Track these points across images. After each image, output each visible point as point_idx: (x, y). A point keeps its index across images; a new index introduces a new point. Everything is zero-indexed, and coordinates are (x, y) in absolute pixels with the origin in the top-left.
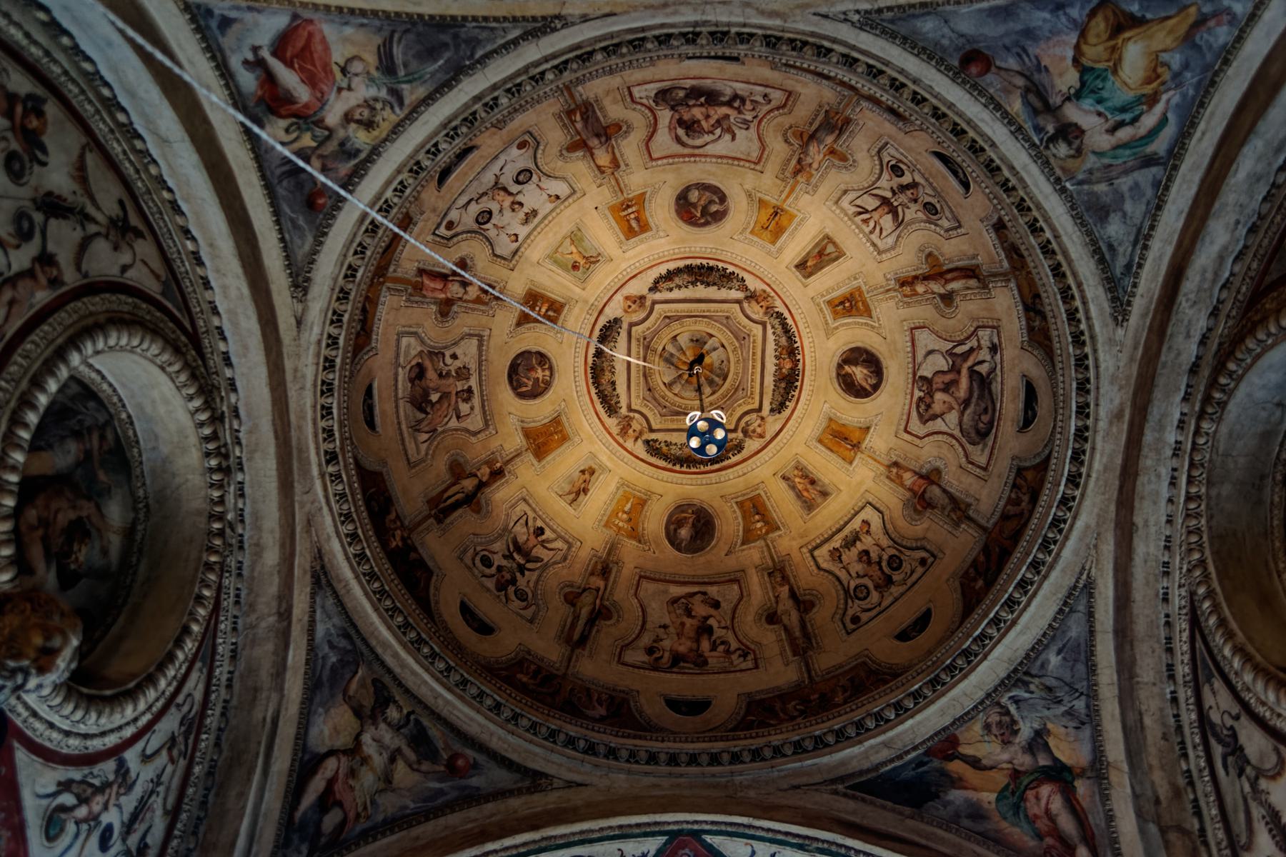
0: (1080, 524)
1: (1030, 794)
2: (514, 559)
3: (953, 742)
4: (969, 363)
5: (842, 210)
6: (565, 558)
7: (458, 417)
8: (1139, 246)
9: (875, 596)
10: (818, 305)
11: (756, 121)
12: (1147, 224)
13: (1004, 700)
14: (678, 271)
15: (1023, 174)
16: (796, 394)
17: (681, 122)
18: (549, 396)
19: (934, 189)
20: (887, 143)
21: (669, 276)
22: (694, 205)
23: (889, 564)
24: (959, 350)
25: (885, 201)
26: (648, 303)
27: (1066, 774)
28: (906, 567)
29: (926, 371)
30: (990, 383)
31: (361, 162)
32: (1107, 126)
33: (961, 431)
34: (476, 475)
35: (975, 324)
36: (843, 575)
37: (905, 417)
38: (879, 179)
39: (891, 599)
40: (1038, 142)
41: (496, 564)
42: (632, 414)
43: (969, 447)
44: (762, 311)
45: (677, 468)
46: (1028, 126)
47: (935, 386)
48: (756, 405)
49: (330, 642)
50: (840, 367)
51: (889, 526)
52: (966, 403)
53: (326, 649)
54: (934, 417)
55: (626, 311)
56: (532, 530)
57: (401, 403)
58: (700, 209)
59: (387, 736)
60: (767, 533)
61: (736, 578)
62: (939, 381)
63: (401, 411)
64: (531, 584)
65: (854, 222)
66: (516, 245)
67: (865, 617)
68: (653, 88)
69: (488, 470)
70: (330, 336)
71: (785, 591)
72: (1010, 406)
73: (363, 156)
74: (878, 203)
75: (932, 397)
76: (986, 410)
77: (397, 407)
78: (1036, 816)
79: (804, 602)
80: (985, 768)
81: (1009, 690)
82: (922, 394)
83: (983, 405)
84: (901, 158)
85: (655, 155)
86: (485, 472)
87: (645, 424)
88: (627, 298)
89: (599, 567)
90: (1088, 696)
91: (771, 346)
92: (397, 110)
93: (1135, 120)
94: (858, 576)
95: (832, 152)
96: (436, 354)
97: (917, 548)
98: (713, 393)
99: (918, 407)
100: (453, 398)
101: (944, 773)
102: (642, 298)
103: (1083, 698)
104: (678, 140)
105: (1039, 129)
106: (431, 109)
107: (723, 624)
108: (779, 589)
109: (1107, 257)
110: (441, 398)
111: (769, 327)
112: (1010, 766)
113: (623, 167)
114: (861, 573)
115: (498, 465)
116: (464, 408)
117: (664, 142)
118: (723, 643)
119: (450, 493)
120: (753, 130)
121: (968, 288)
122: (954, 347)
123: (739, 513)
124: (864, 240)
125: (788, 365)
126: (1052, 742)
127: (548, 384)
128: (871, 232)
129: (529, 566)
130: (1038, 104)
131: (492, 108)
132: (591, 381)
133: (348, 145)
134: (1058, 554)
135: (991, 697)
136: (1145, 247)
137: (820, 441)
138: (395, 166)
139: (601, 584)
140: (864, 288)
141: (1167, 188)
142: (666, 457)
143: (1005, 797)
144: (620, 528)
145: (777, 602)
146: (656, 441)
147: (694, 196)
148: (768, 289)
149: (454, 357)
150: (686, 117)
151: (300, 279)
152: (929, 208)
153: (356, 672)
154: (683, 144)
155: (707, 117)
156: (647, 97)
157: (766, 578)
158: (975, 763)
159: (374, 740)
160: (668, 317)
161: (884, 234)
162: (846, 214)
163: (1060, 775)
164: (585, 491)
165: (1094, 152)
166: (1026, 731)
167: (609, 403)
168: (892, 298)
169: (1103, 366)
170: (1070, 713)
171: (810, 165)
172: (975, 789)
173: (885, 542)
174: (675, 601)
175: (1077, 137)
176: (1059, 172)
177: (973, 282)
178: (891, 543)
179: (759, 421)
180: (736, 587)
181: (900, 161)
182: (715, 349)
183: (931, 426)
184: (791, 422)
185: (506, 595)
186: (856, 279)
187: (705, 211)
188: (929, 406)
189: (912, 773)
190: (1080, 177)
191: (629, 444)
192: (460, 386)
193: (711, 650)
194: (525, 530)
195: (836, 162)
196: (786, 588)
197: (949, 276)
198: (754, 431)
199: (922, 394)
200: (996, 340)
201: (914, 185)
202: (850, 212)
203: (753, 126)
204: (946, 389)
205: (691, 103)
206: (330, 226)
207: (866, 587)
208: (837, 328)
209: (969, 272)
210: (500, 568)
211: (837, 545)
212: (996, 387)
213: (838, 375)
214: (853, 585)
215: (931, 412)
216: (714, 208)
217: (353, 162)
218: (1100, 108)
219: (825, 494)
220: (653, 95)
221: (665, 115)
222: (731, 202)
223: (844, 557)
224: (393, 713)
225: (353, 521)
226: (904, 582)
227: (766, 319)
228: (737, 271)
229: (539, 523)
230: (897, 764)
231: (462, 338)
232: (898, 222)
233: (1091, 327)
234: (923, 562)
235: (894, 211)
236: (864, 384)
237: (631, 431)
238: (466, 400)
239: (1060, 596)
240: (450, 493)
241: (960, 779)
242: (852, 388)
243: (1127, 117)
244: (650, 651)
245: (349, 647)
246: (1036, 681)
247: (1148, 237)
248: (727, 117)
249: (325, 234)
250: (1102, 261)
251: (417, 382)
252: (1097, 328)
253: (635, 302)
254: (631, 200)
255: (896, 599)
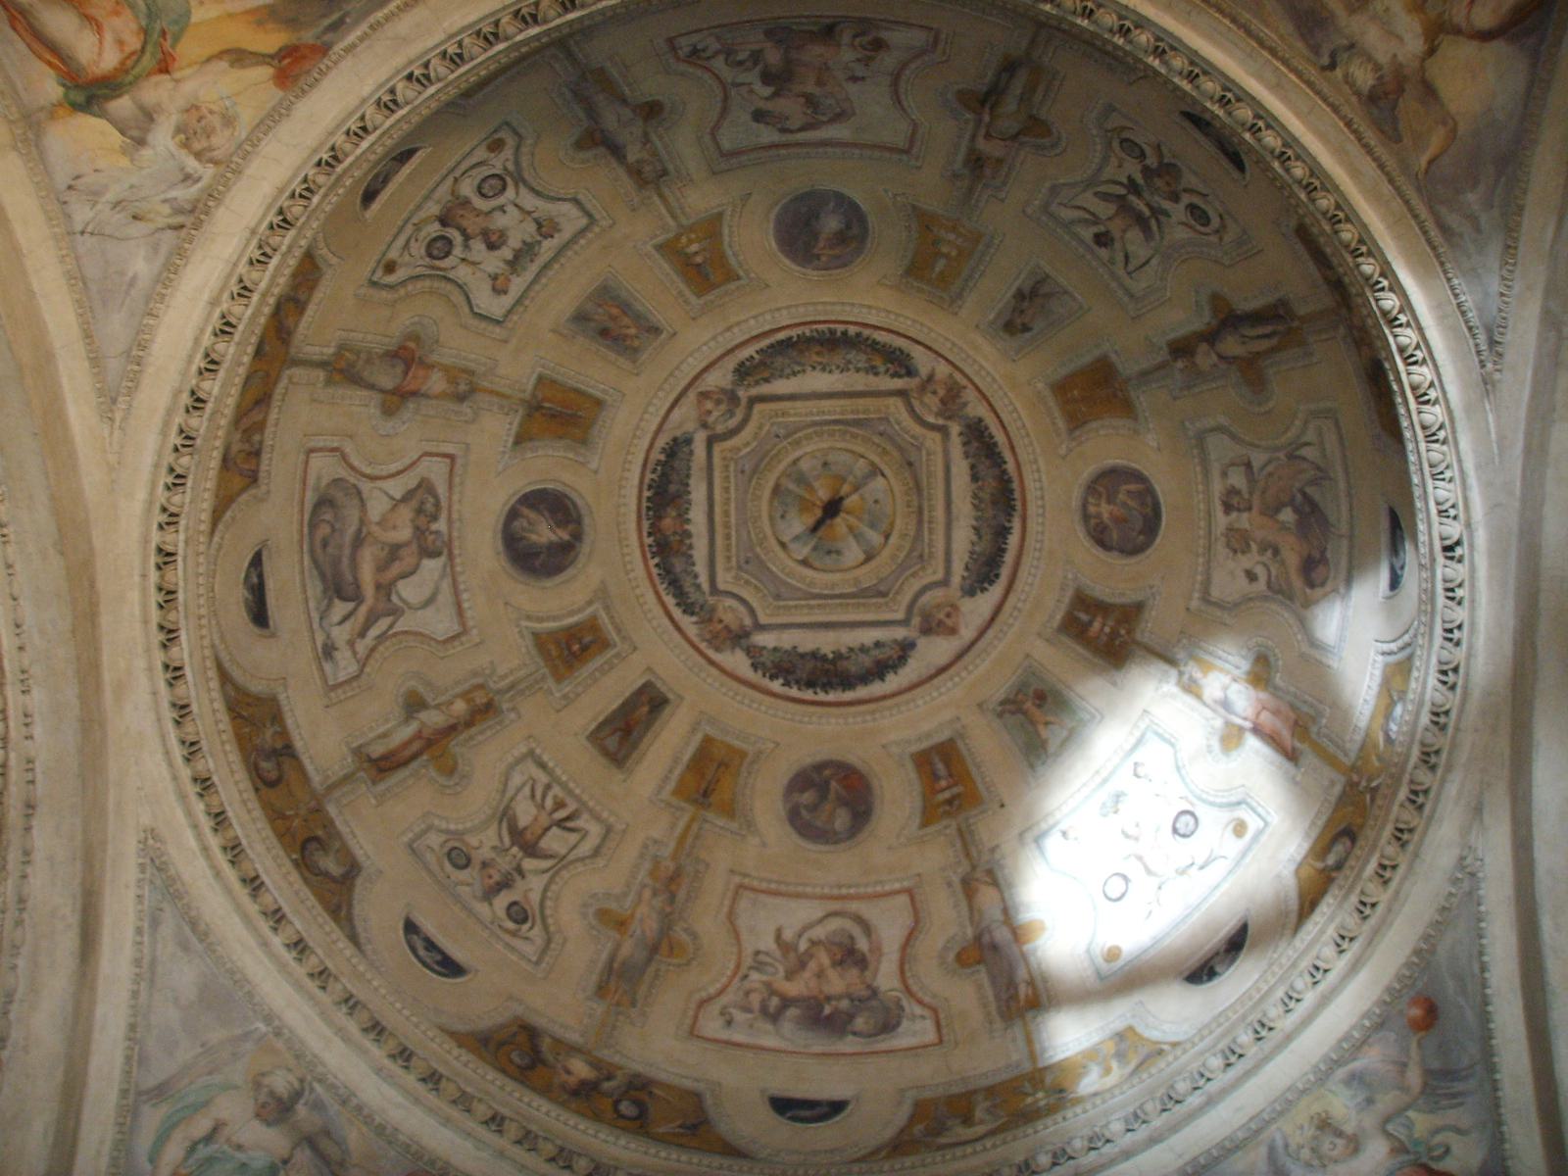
0: (141, 495)
1: (134, 43)
2: (1148, 205)
3: (283, 79)
4: (363, 609)
5: (597, 818)
6: (1054, 190)
7: (1248, 465)
8: (146, 961)
9: (467, 189)
10: (624, 639)
11: (743, 970)
12: (144, 995)
13: (208, 172)
14: (865, 678)
15: (328, 1032)
16: (649, 476)
17: (862, 963)
18: (1088, 471)
19: (457, 899)
20: (537, 963)
21: (880, 670)
22: (843, 802)
23: (449, 242)
24: (382, 624)
25: (531, 850)
26: (916, 621)
27: (80, 98)
28: (418, 249)
29: (431, 567)
30: (325, 591)
31: (1346, 1063)
32: (226, 1131)
33: (359, 493)
34: (1221, 357)
35: (364, 677)
36: (529, 201)
37: (457, 480)
38: (546, 890)
39: (437, 195)
40: (316, 1085)
41: (1181, 206)
42: (941, 422)
43: (342, 472)
44: (720, 614)
45: (852, 330)
46: (334, 1107)
47: (414, 547)
48: (717, 448)
49: (1478, 230)
50: (578, 536)
51: (457, 297)
52: (358, 541)
53: (1484, 219)
54: (406, 498)
55: (955, 607)
56: (1117, 245)
57: (1344, 528)
58: (832, 796)
59: (1372, 37)
60: (678, 237)
61: (725, 161)
62: (408, 558)
63: (1344, 508)
64: (1114, 161)
65: (578, 799)
66: (1137, 756)
67: (481, 154)
68: (903, 1039)
69: (1199, 359)
70: (1433, 768)
71: (633, 154)
72: (291, 583)
73: (1341, 1073)
74: (544, 844)
75: (417, 528)
76: (325, 545)
77: (1352, 527)
78: (117, 13)
79: (595, 144)
80: (220, 55)
81: (202, 190)
82: (434, 527)
83: (330, 550)
84: (518, 943)
85: (904, 899)
86: (1205, 358)
87: (916, 404)
88: (953, 631)
89: (988, 172)
90: (71, 233)
91: (700, 553)
92: (1279, 1143)
93: (192, 1149)
94: (502, 209)
95: (621, 924)
96: (1280, 592)
97: (403, 283)
98: (795, 462)
99: (437, 505)
100: (1256, 502)
101: (292, 23)
102: (927, 630)
103: (79, 228)
104: (867, 928)
105: (318, 1106)
106: (1226, 1131)
107: (744, 90)
108: (645, 155)
109: (187, 929)
110: (1277, 510)
111: (706, 586)
112: (177, 75)
113: (956, 880)
114: (497, 214)
115: (1180, 364)
116: (1238, 479)
117: (890, 925)
118: (740, 63)
119: (1265, 344)
120: (748, 951)
121: (384, 735)
122: (391, 627)
123: (733, 261)
124: (558, 771)
125: (667, 523)
126: (116, 138)
127: (1092, 488)
128: (548, 787)
129: (1123, 191)
130: (326, 1145)
131: (1136, 1116)
132: (1015, 485)
133: (1361, 1097)
134: (164, 433)
135: (230, 168)
136: (138, 962)
137: (599, 403)
138: (1294, 1045)
139: (981, 144)
140: (550, 683)
141: (128, 1059)
142: (875, 347)
143: (176, 22)
144: (954, 229)
145: (646, 134)
146: (896, 375)
147: (842, 820)
148: (711, 653)
149: (1251, 576)
150: (853, 973)
151: (1466, 885)
152: (459, 858)
153: (1430, 162)
154: (859, 920)
155: (820, 975)
156: (913, 1018)
157: (671, 167)
158: (239, 57)
159: (1400, 38)
160: (884, 595)
161: (527, 790)
162: (591, 811)
163: (90, 93)
164: (1020, 295)
165: (236, 1087)
166: (163, 138)
167: (982, 445)
168: (505, 677)
169: (159, 756)
170: (94, 195)
171: (655, 893)
172: (230, 16)
173: (463, 273)
174: (839, 117)
175: (263, 1106)
176: (279, 1044)
177: (377, 750)
178: (451, 275)
179: (711, 420)
180: (726, 145)
181: (514, 934)
182: (797, 538)
183: (410, 481)
184: (654, 427)
185: (1161, 155)
186: (565, 697)
187: (823, 789)
188: (419, 511)
189: (348, 8)
190: (249, 1046)
191: (942, 370)
192: (1243, 521)
193: (761, 51)
194: (1131, 248)
195: (613, 906)
196: (631, 158)
197: (416, 746)
198: (718, 402)
199: (434, 527)
200: (328, 667)
201: (490, 893)
202: (585, 816)
203: (748, 961)
204: (394, 551)
205: (845, 1004)
206: (1408, 965)
207: (483, 195)
208: (590, 603)
209: (383, 765)
210: (1175, 198)
211: (547, 244)
212: (315, 588)
213: (579, 522)
214: (510, 193)
215: (414, 503)
216: (808, 797)
217: (1356, 1065)
218: (241, 1156)
219: (581, 318)
220: (905, 1024)
221: (886, 978)
222: (780, 808)
223: (532, 227)
224: (1364, 78)
225: (1424, 428)
226: (418, 227)
227: (711, 600)
228: (766, 682)
229: (1103, 253)
230: (379, 15)
231: (1236, 605)
232: (506, 815)
233: (189, 814)
234: (390, 268)
235: (517, 834)
236: (532, 515)
237: (942, 392)
238: (1233, 491)
239: (151, 370)
240: (1265, 344)
241: (260, 24)
242: (555, 505)
243: (203, 1152)
244: (878, 45)
245: (1443, 211)
246: (161, 222)
247: (137, 979)
248: (790, 975)
249: (1417, 952)
250: (194, 924)
251: (1316, 555)
252: (179, 813)
253: (940, 623)
254: (948, 814)
255: (427, 198)
